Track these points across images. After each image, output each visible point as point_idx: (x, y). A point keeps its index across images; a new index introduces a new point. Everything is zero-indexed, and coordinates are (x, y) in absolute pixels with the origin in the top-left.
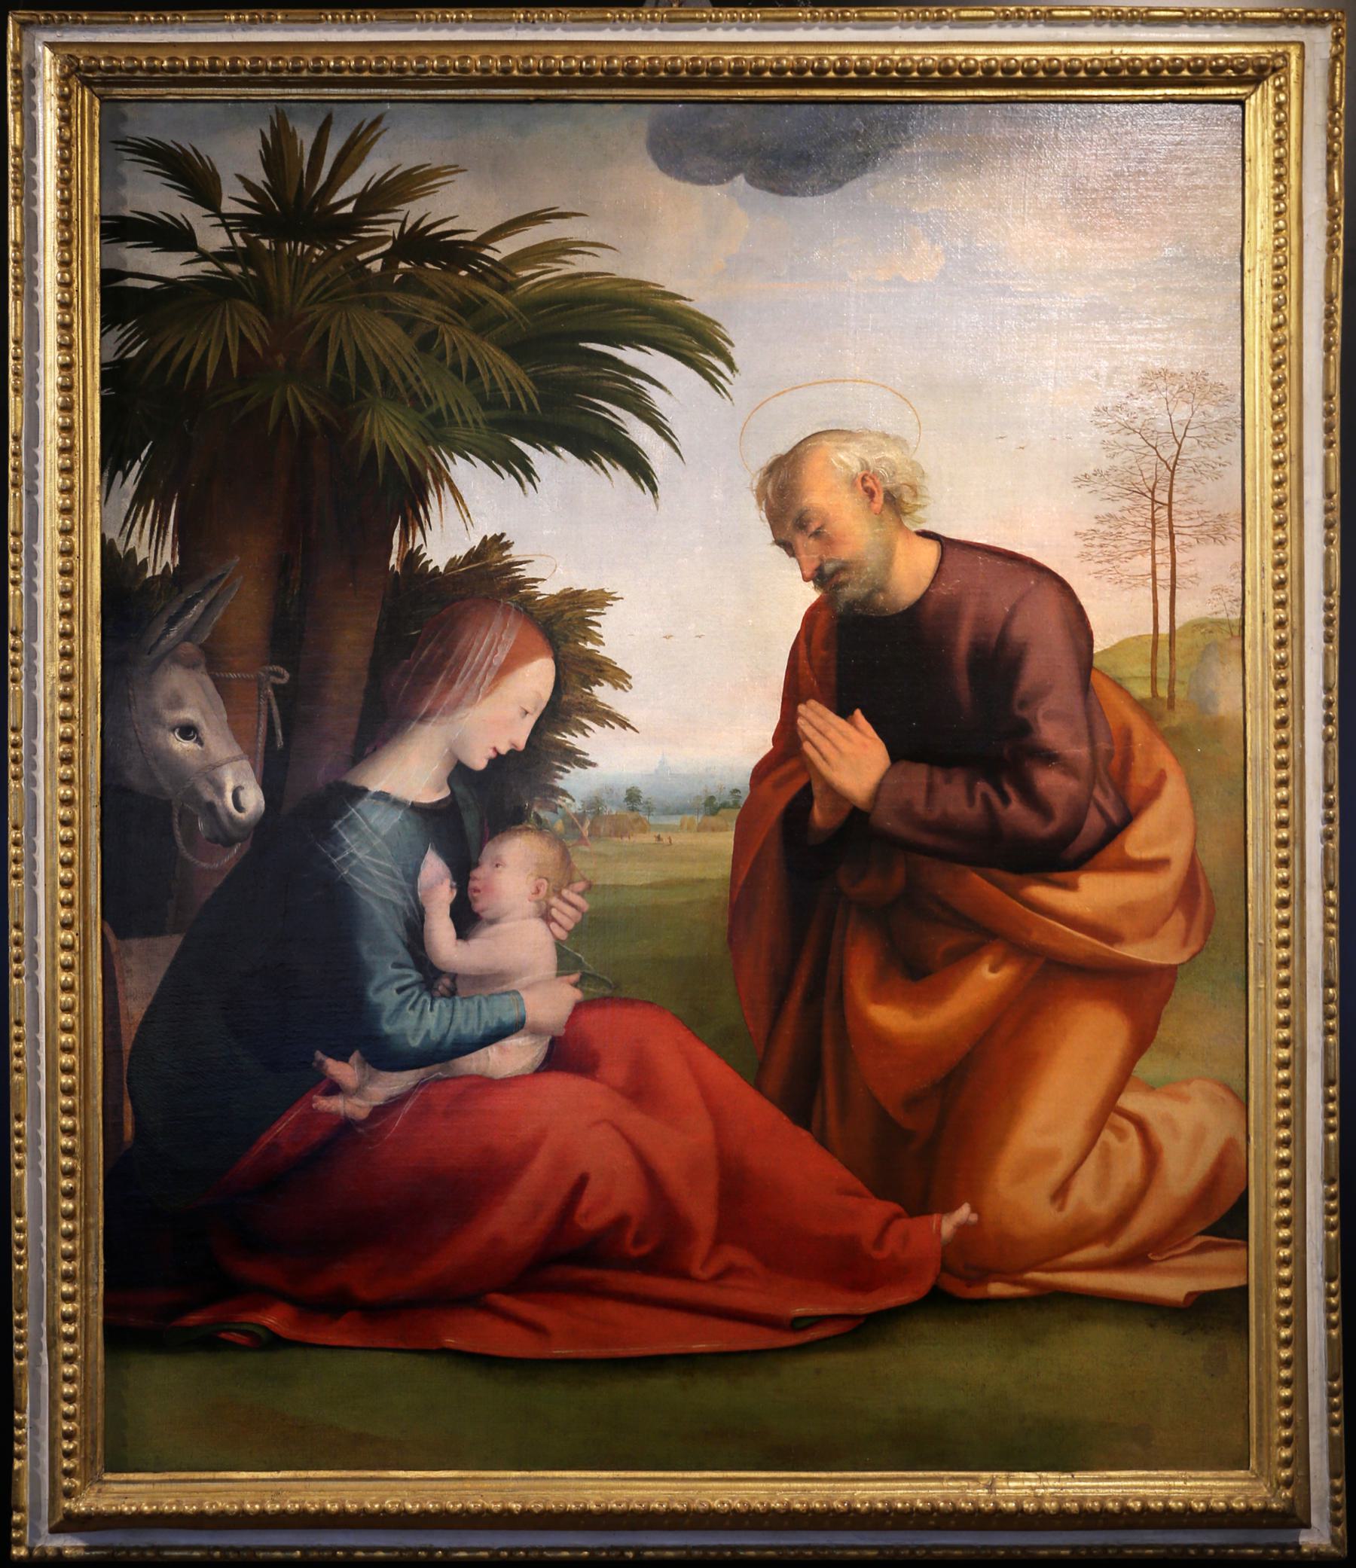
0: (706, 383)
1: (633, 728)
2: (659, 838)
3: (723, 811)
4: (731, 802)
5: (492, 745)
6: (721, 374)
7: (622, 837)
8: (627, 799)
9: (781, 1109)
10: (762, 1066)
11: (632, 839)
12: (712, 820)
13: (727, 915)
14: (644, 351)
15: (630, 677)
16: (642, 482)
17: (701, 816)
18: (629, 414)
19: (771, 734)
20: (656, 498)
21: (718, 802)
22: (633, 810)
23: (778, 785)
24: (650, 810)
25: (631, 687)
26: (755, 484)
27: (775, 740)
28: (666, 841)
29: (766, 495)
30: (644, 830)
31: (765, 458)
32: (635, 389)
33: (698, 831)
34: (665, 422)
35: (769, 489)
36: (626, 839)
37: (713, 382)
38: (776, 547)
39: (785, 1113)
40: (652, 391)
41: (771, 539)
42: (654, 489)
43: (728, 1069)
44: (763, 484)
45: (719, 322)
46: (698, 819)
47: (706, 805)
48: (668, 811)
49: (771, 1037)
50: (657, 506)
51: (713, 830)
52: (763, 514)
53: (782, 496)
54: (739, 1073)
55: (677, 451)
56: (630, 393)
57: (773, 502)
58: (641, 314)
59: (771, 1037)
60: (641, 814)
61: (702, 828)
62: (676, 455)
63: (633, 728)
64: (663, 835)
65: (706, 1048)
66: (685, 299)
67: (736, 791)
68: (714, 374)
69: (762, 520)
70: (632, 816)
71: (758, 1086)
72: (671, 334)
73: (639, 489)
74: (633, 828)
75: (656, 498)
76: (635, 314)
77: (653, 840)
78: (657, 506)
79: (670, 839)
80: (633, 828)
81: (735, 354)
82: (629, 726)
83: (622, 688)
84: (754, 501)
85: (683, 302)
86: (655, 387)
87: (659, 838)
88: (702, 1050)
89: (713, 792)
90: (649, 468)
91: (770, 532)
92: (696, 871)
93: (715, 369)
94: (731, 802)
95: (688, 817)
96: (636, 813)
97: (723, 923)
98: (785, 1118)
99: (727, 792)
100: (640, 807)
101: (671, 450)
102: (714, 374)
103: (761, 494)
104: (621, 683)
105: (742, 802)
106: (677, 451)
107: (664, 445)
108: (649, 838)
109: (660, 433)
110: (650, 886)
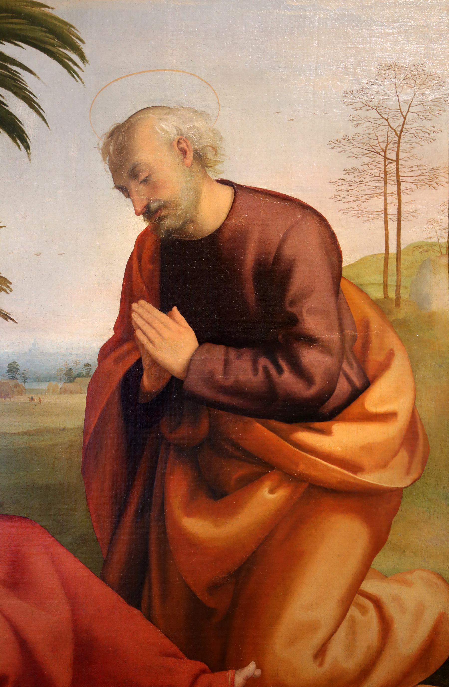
0: (65, 70)
1: (13, 320)
2: (32, 399)
3: (78, 380)
4: (84, 372)
5: (18, 324)
6: (75, 64)
7: (5, 398)
8: (9, 371)
9: (120, 594)
10: (106, 563)
11: (12, 399)
12: (71, 386)
13: (81, 454)
14: (19, 46)
15: (11, 283)
16: (19, 142)
17: (62, 383)
18: (9, 93)
19: (113, 324)
20: (29, 154)
21: (75, 373)
22: (13, 378)
23: (118, 361)
24: (25, 378)
25: (11, 290)
26: (101, 145)
27: (116, 328)
28: (37, 401)
29: (109, 153)
30: (21, 393)
31: (108, 127)
32: (13, 74)
33: (60, 393)
34: (35, 99)
35: (111, 148)
36: (8, 399)
37: (70, 70)
38: (117, 191)
39: (122, 597)
40: (25, 76)
41: (112, 184)
42: (27, 147)
43: (81, 565)
44: (107, 145)
45: (74, 25)
46: (61, 385)
47: (66, 375)
48: (39, 379)
49: (112, 541)
50: (30, 160)
51: (71, 393)
52: (107, 167)
53: (120, 153)
54: (89, 568)
55: (44, 120)
56: (10, 77)
57: (113, 158)
58: (16, 18)
59: (112, 541)
60: (19, 382)
61: (63, 392)
62: (43, 123)
63: (13, 320)
64: (36, 397)
65: (65, 550)
66: (48, 7)
67: (88, 365)
68: (70, 64)
69: (106, 171)
70: (12, 383)
71: (103, 578)
72: (39, 34)
73: (17, 147)
74: (13, 392)
75: (29, 154)
76: (12, 18)
77: (28, 400)
78: (30, 160)
79: (40, 399)
80: (13, 392)
81: (85, 48)
82: (10, 318)
83: (5, 291)
84: (100, 157)
85: (46, 10)
86: (27, 73)
87: (32, 399)
88: (62, 551)
89: (71, 366)
90: (23, 132)
91: (112, 179)
92: (59, 423)
93: (71, 60)
94: (84, 372)
95: (53, 383)
96: (15, 381)
97: (78, 459)
98: (122, 600)
99: (81, 366)
100: (18, 377)
101: (40, 119)
102: (70, 64)
103: (105, 152)
104: (4, 287)
105: (92, 373)
106: (44, 120)
107: (35, 115)
108: (25, 399)
109: (32, 106)
110: (25, 433)
